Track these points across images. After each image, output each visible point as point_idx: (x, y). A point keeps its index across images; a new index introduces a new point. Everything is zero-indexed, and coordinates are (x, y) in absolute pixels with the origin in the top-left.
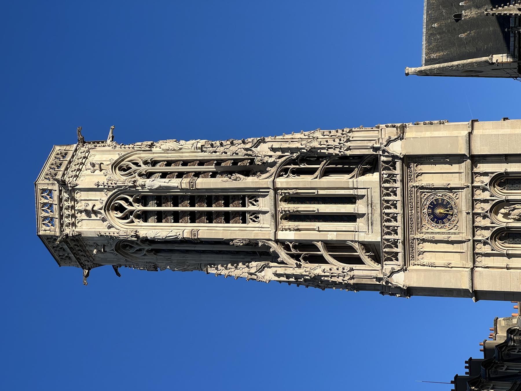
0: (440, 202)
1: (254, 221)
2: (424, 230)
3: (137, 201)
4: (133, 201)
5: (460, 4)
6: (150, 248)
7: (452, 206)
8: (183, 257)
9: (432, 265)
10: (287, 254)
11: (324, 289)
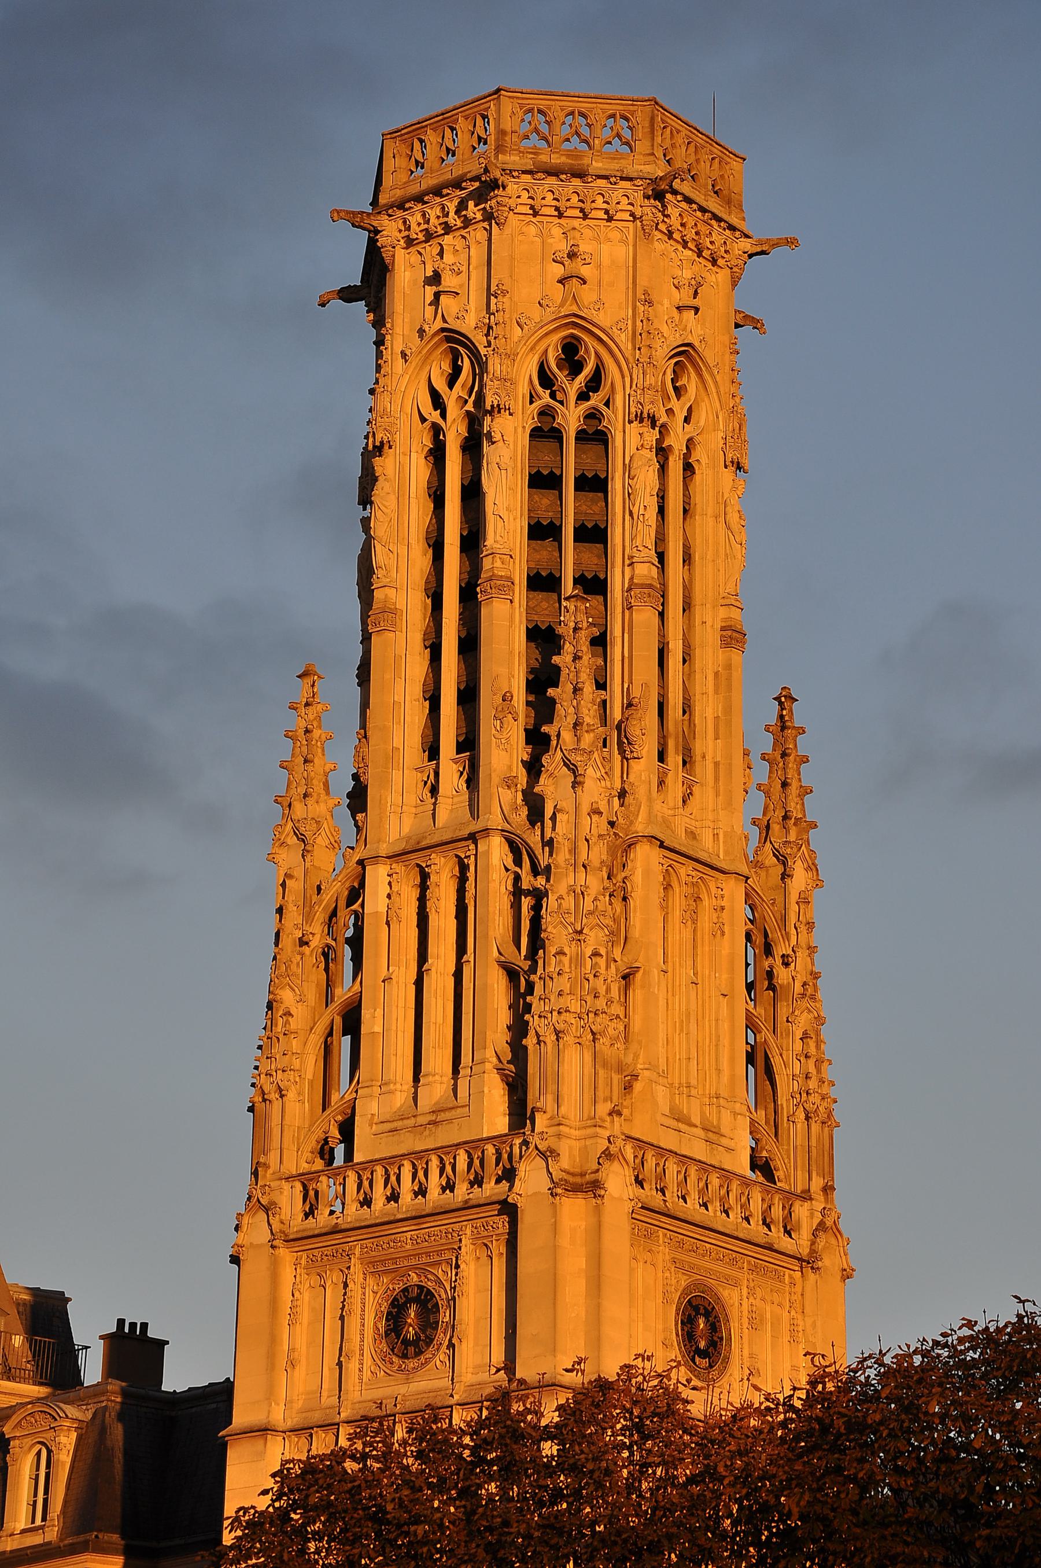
2: (371, 1281)
7: (422, 1352)
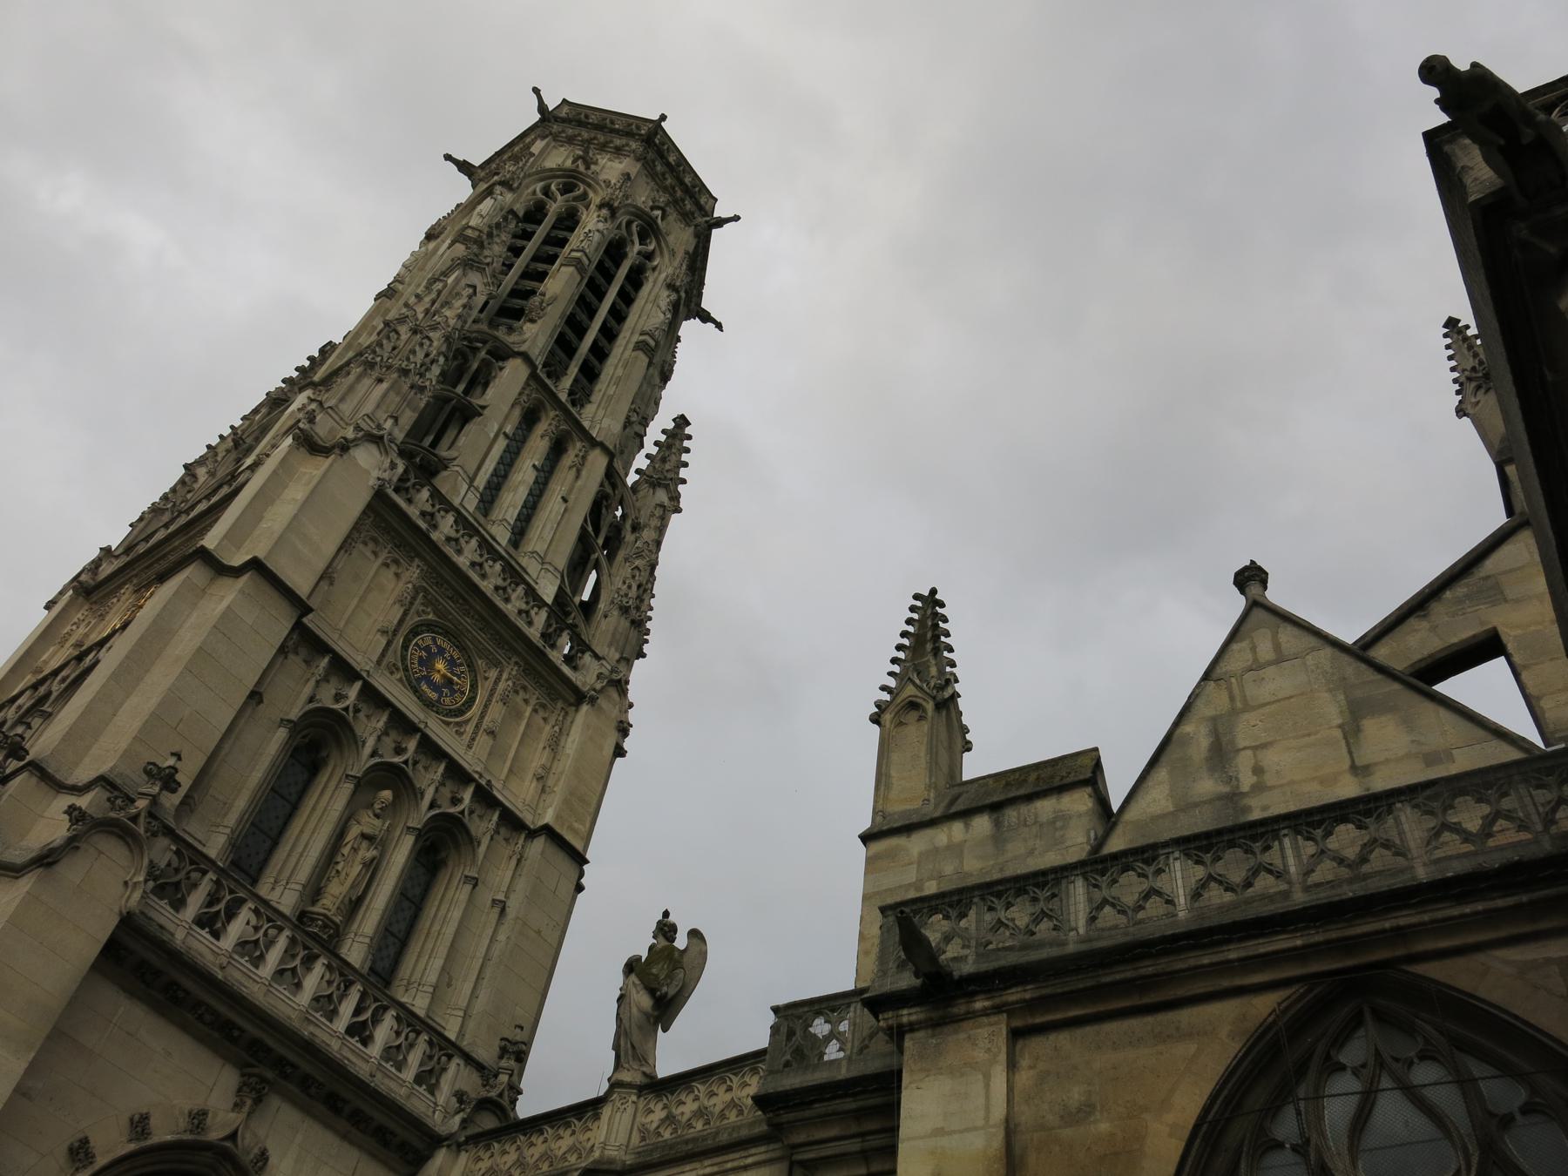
4: (644, 265)
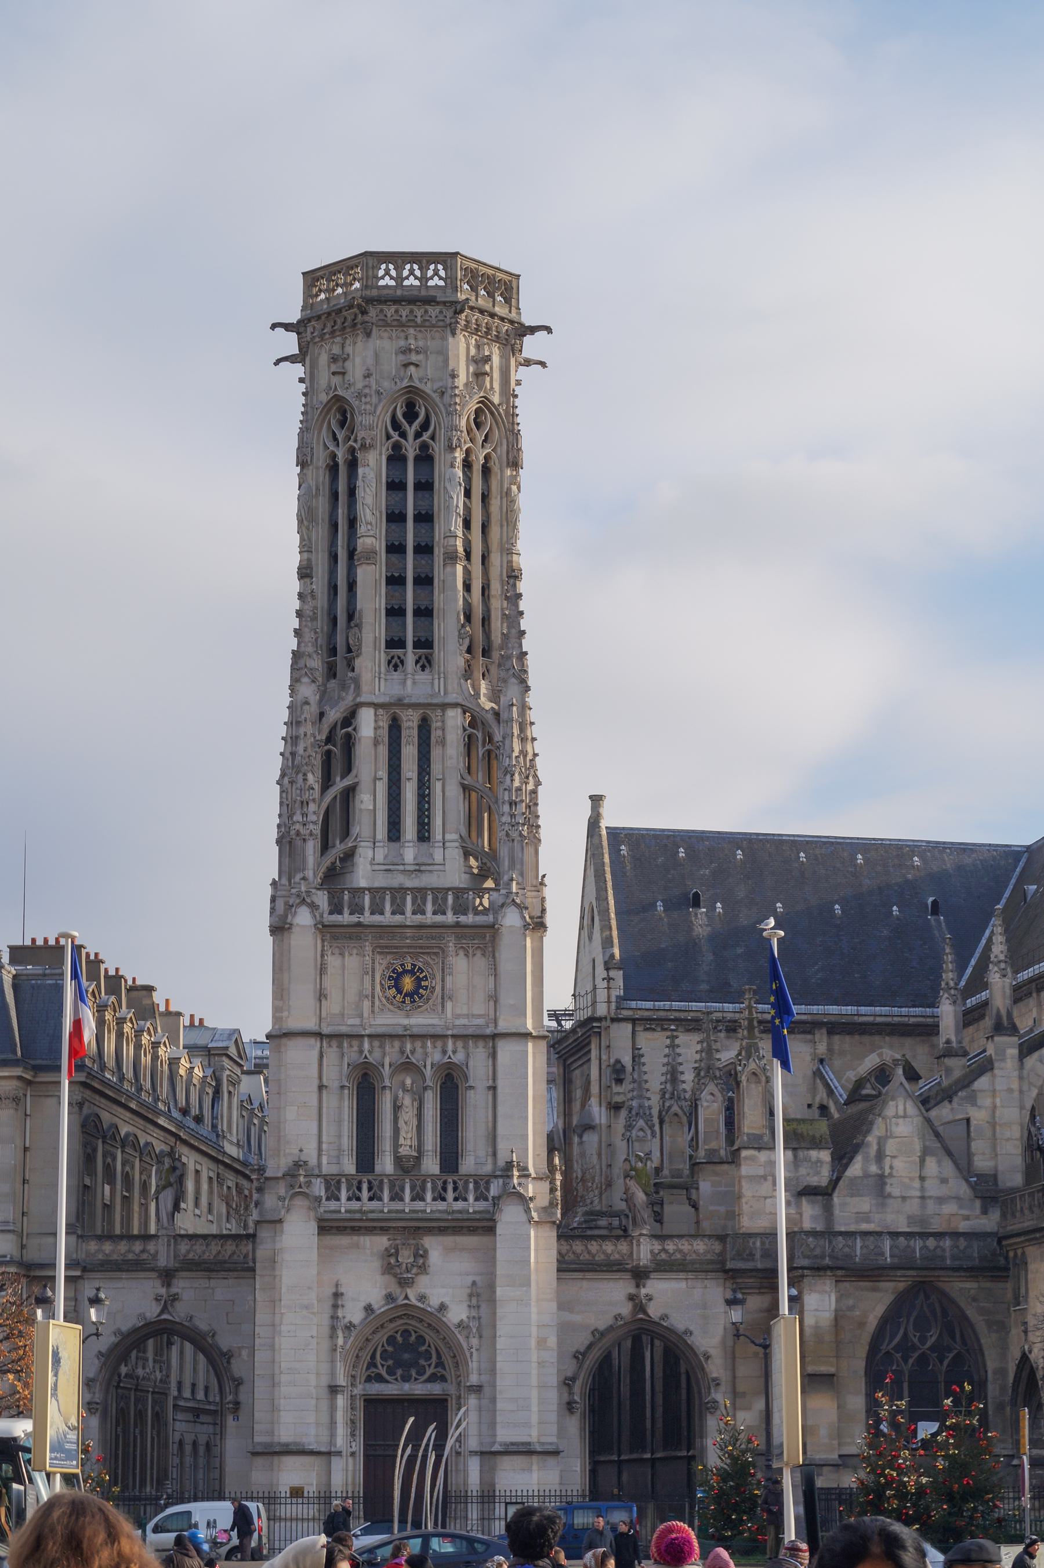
0: (423, 983)
1: (389, 662)
2: (378, 957)
3: (424, 447)
4: (424, 441)
5: (719, 905)
6: (340, 460)
8: (323, 520)
9: (322, 970)
10: (336, 723)
11: (278, 783)
